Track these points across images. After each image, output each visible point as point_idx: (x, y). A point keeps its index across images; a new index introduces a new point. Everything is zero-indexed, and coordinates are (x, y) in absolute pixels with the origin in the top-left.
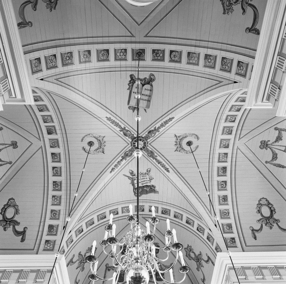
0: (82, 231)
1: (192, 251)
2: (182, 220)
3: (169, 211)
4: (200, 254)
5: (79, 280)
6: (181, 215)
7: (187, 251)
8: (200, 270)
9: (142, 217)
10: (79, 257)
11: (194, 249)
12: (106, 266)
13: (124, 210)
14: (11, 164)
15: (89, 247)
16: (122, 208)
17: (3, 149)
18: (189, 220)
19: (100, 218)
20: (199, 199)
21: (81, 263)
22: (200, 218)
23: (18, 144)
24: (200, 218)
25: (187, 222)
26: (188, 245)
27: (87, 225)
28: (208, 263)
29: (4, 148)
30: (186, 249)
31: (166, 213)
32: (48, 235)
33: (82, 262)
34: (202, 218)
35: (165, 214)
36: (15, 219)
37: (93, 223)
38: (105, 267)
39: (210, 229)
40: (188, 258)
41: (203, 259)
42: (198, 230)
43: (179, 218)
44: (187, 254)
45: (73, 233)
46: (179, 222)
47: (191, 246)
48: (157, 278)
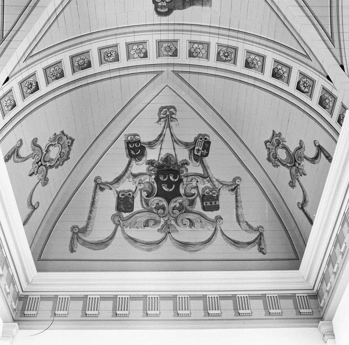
0: (37, 88)
1: (283, 144)
2: (262, 71)
3: (233, 51)
4: (301, 147)
5: (38, 203)
6: (262, 59)
7: (271, 147)
8: (297, 184)
9: (173, 71)
10: (33, 150)
11: (286, 140)
12: (95, 181)
13: (132, 52)
15: (55, 134)
16: (128, 45)
18: (279, 67)
19: (76, 64)
20: (306, 9)
21: (39, 166)
22: (307, 56)
24: (307, 55)
25: (275, 75)
26: (274, 131)
27: (48, 75)
28: (317, 161)
30: (269, 143)
31: (227, 59)
33: (41, 165)
34: (311, 56)
35: (225, 61)
37: (62, 75)
38: (93, 184)
39: (328, 78)
40: (271, 164)
41: (305, 157)
42: (298, 88)
43: (257, 66)
44: (269, 155)
45: (14, 84)
46: (255, 79)
47: (280, 133)
48: (205, 205)
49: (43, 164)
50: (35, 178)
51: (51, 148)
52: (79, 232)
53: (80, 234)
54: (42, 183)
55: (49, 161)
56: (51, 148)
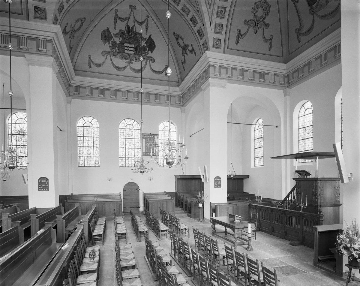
14: (149, 17)
15: (252, 8)
17: (134, 17)
21: (258, 26)
23: (133, 5)
29: (134, 16)
32: (201, 39)
36: (185, 44)
49: (257, 23)
50: (260, 31)
51: (256, 14)
52: (299, 31)
53: (300, 32)
54: (266, 28)
55: (261, 18)
56: (256, 14)
